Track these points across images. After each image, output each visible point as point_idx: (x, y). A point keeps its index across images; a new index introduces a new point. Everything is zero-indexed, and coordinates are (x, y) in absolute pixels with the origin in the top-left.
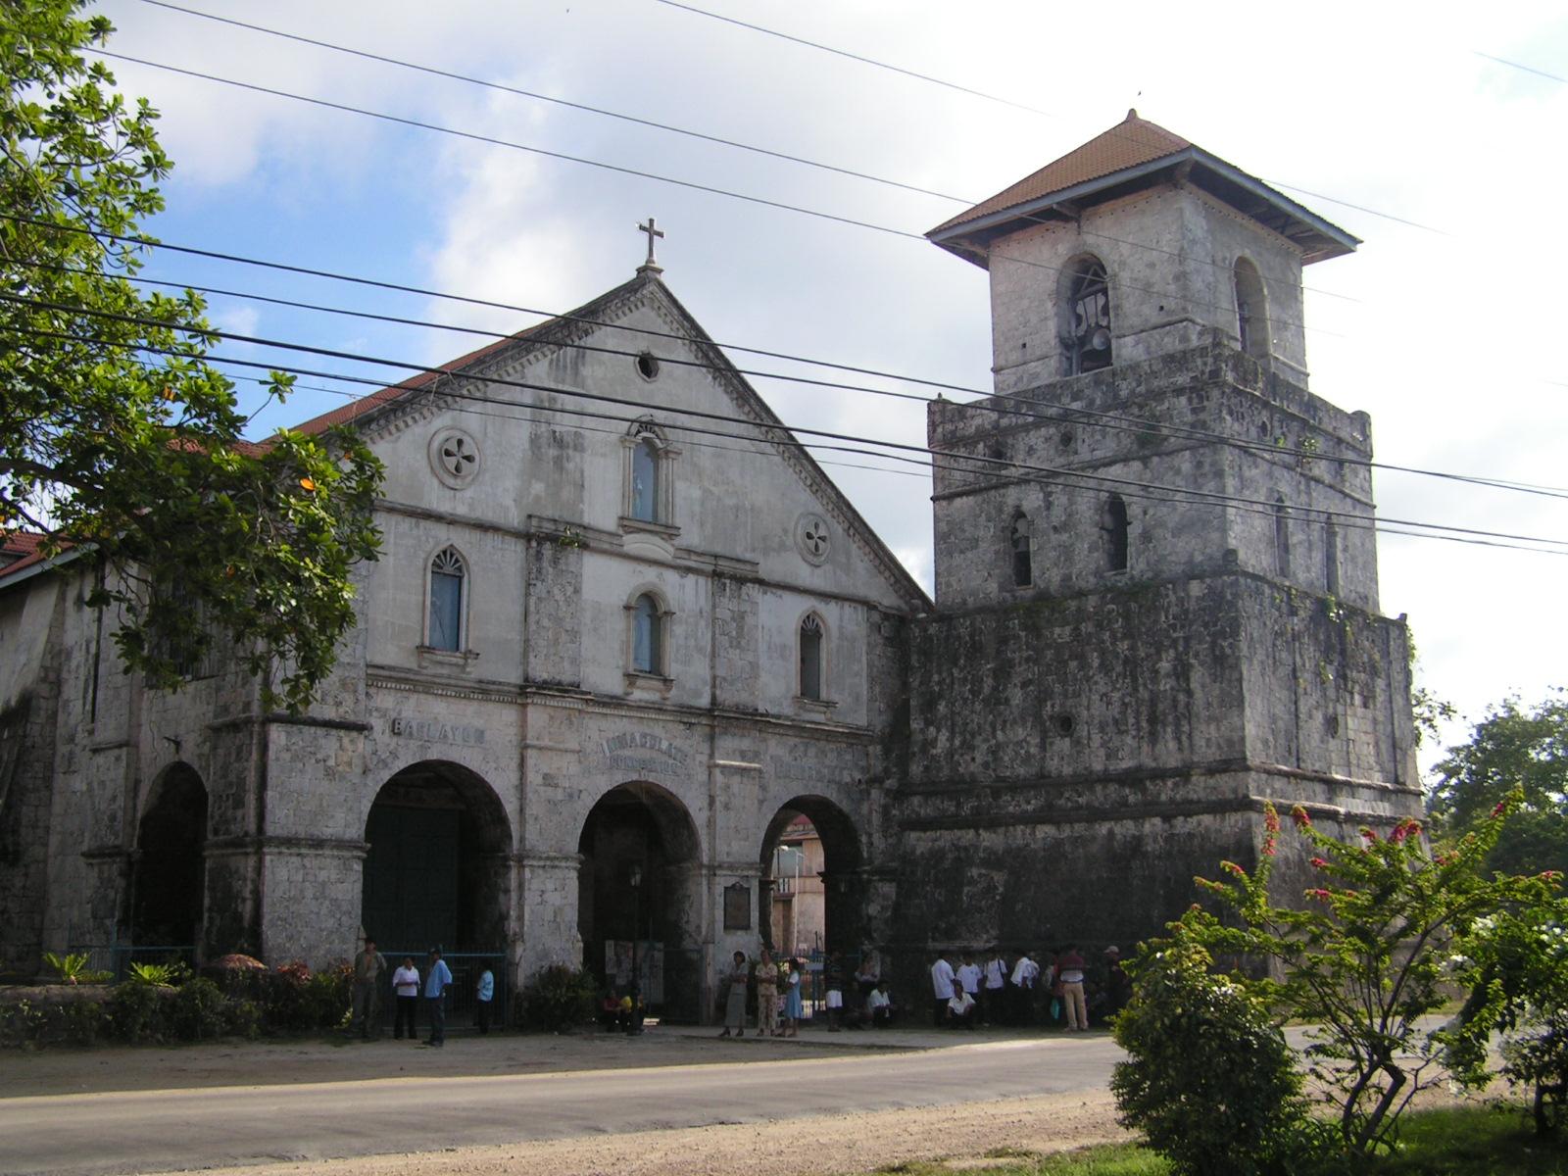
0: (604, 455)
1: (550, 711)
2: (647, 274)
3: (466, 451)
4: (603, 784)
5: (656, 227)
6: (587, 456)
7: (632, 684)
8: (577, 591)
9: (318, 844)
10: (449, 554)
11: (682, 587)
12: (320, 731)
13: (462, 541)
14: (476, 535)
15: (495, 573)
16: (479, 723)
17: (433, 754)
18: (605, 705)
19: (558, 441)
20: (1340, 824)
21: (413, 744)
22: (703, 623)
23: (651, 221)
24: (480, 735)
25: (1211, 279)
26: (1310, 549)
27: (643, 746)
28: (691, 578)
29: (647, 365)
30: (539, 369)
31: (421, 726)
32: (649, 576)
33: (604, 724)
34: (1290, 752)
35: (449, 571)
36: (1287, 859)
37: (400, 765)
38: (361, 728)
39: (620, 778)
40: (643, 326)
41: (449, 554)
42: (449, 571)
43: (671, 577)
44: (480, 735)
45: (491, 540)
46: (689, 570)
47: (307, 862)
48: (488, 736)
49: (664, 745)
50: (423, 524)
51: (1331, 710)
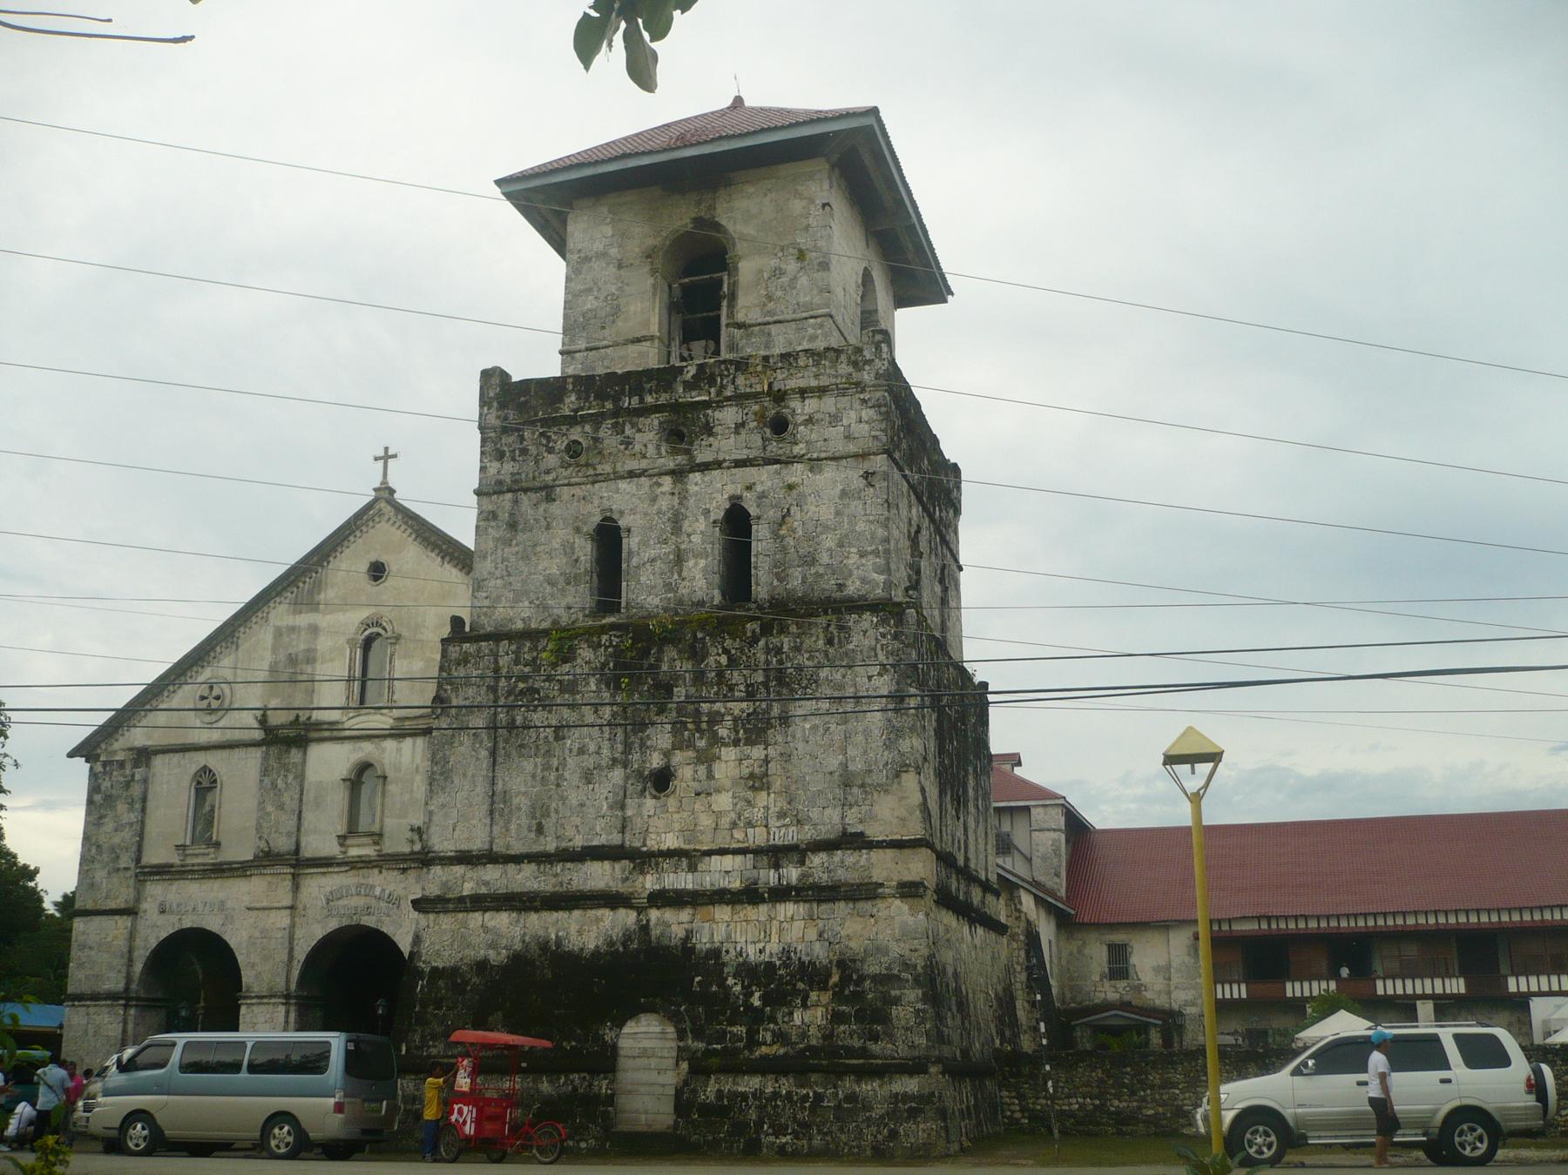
0: (332, 660)
1: (269, 878)
2: (385, 493)
3: (216, 692)
4: (319, 932)
5: (382, 454)
6: (318, 666)
7: (341, 845)
8: (301, 777)
9: (95, 997)
10: (205, 770)
11: (399, 750)
12: (104, 918)
13: (212, 760)
14: (225, 754)
15: (241, 776)
16: (221, 895)
17: (187, 923)
18: (321, 866)
19: (292, 660)
20: (640, 910)
21: (174, 918)
22: (418, 778)
23: (386, 449)
24: (222, 903)
25: (613, 289)
26: (679, 559)
27: (358, 894)
28: (409, 741)
29: (377, 571)
30: (280, 615)
31: (179, 905)
32: (366, 750)
33: (323, 881)
34: (540, 830)
35: (205, 785)
36: (482, 966)
37: (164, 935)
38: (130, 912)
39: (333, 925)
40: (385, 539)
41: (205, 770)
42: (205, 785)
43: (390, 744)
44: (222, 903)
45: (238, 754)
46: (403, 736)
47: (92, 1010)
48: (229, 904)
49: (378, 891)
50: (188, 755)
51: (656, 761)
